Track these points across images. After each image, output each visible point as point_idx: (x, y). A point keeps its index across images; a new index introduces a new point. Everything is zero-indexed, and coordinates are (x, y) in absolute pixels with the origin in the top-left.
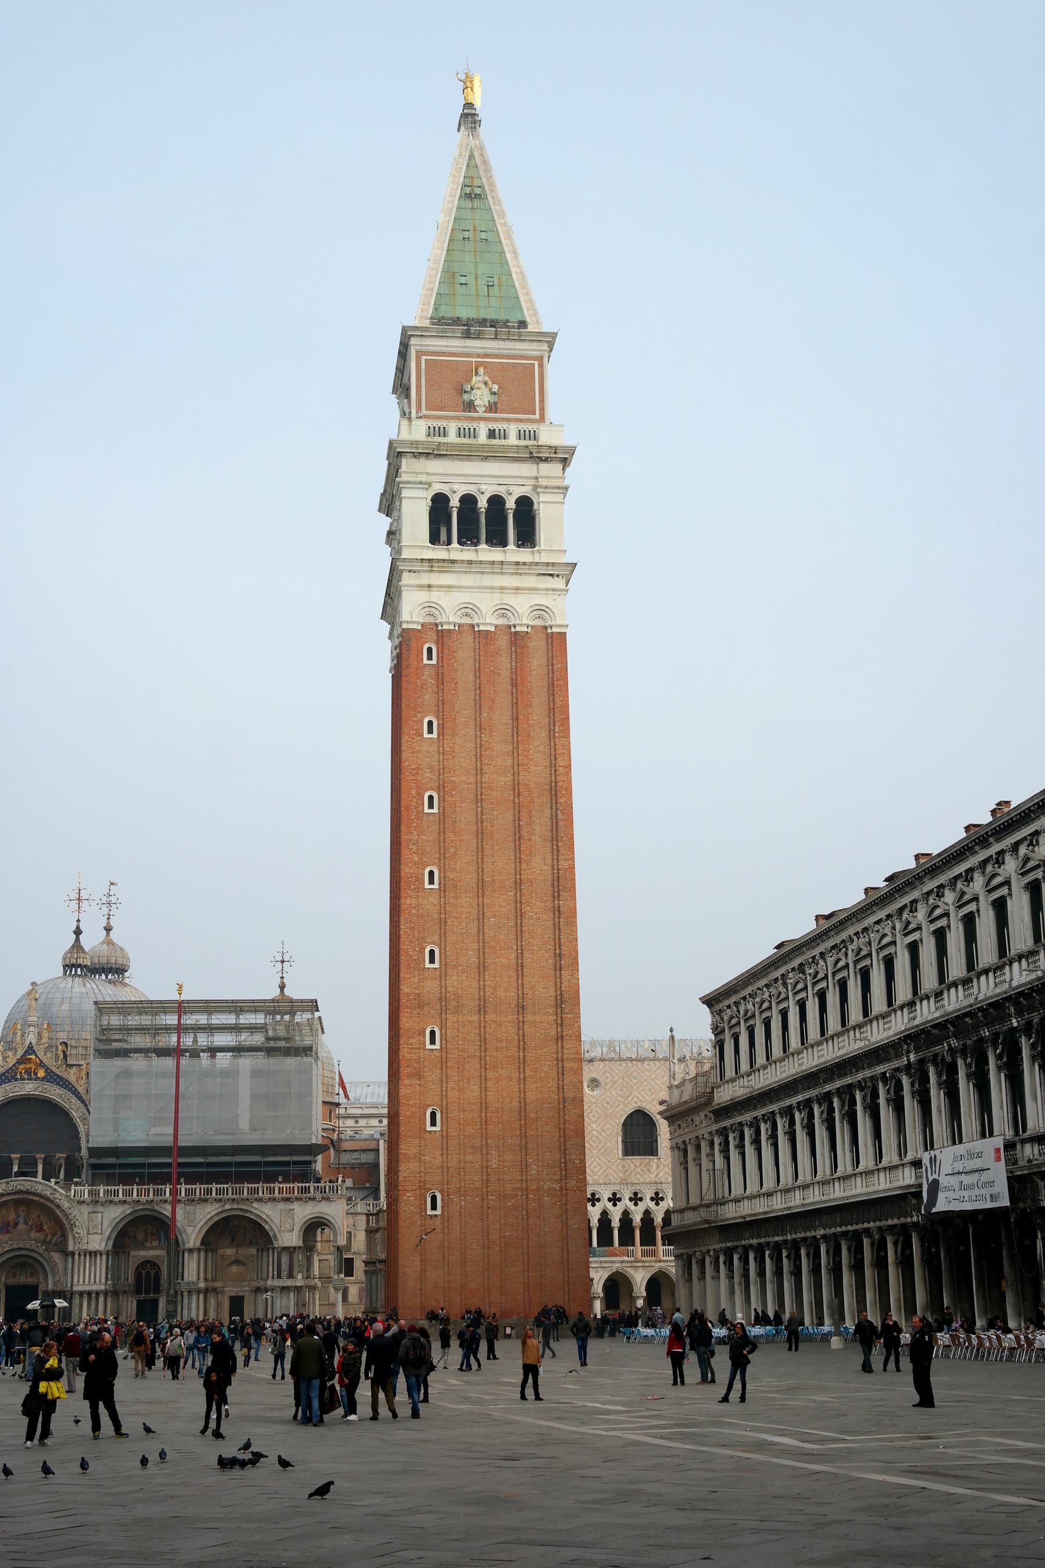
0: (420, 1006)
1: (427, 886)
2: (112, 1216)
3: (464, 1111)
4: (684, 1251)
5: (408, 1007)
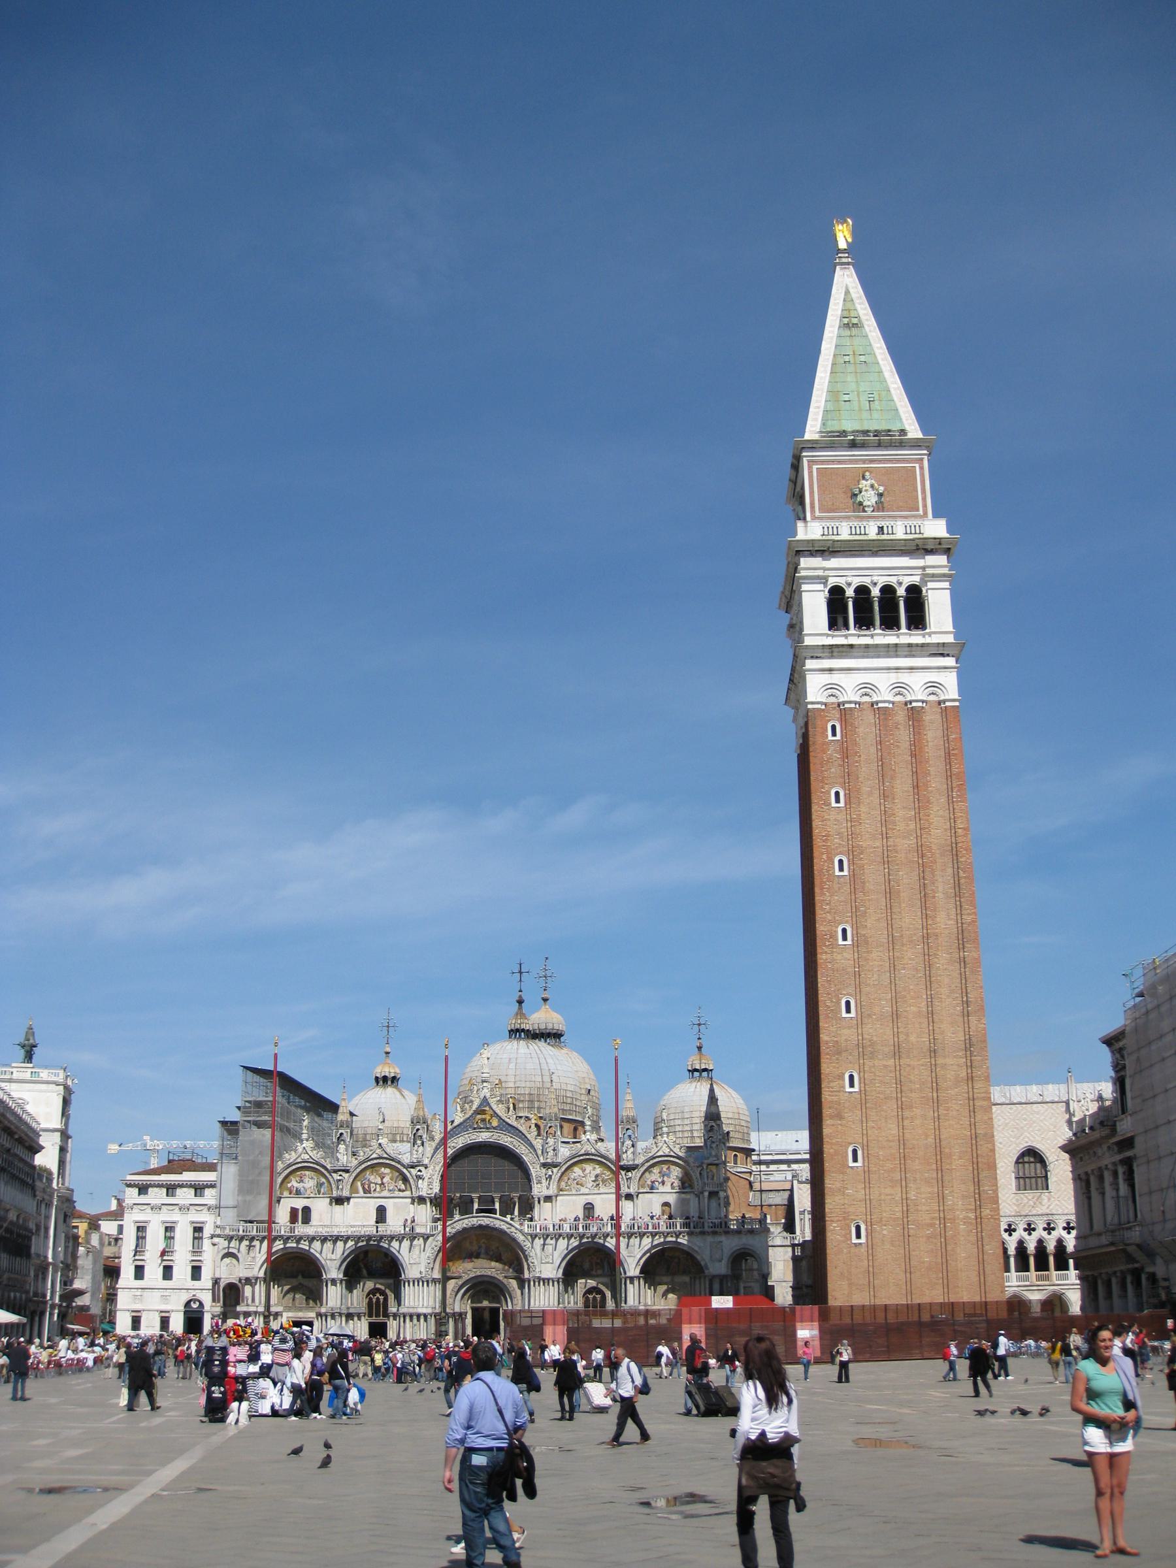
0: (839, 1053)
1: (841, 942)
4: (1089, 1273)
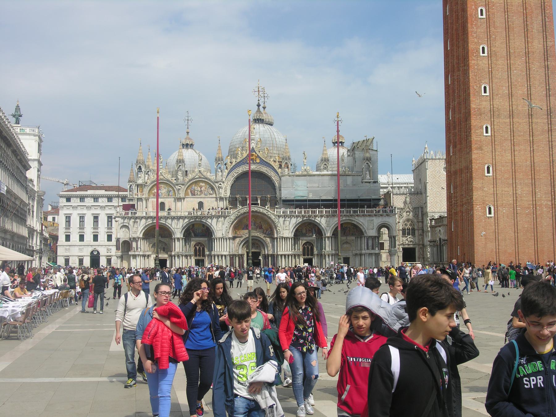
0: (481, 115)
1: (481, 54)
2: (294, 221)
3: (503, 166)
5: (475, 115)
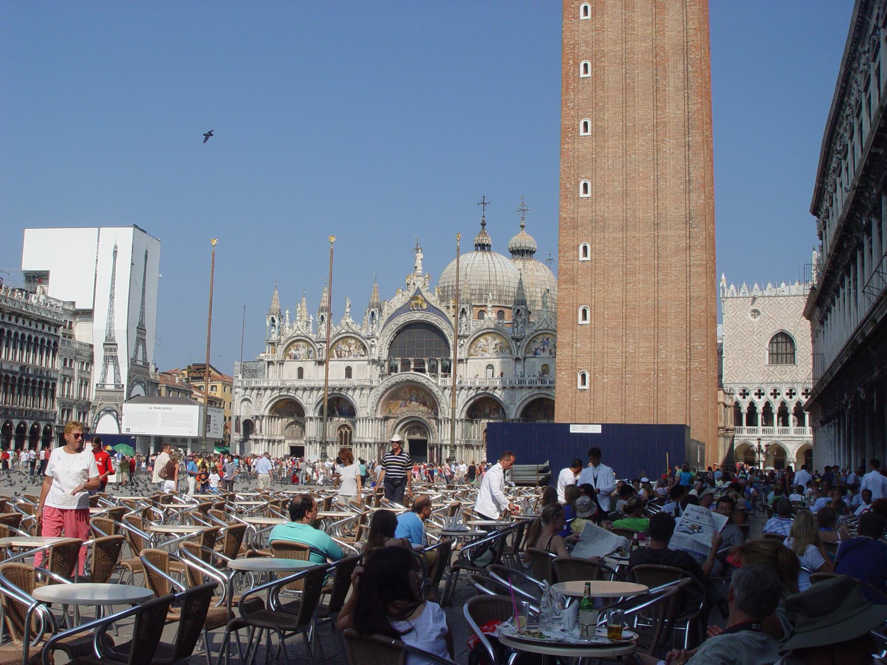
0: (575, 227)
1: (582, 133)
